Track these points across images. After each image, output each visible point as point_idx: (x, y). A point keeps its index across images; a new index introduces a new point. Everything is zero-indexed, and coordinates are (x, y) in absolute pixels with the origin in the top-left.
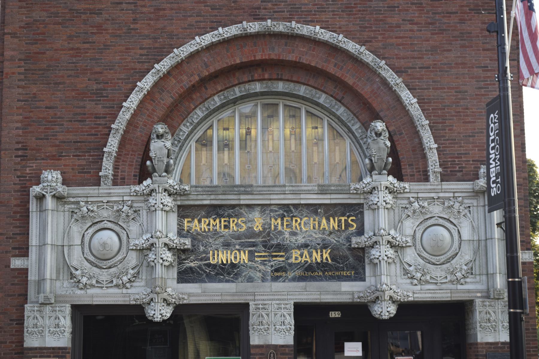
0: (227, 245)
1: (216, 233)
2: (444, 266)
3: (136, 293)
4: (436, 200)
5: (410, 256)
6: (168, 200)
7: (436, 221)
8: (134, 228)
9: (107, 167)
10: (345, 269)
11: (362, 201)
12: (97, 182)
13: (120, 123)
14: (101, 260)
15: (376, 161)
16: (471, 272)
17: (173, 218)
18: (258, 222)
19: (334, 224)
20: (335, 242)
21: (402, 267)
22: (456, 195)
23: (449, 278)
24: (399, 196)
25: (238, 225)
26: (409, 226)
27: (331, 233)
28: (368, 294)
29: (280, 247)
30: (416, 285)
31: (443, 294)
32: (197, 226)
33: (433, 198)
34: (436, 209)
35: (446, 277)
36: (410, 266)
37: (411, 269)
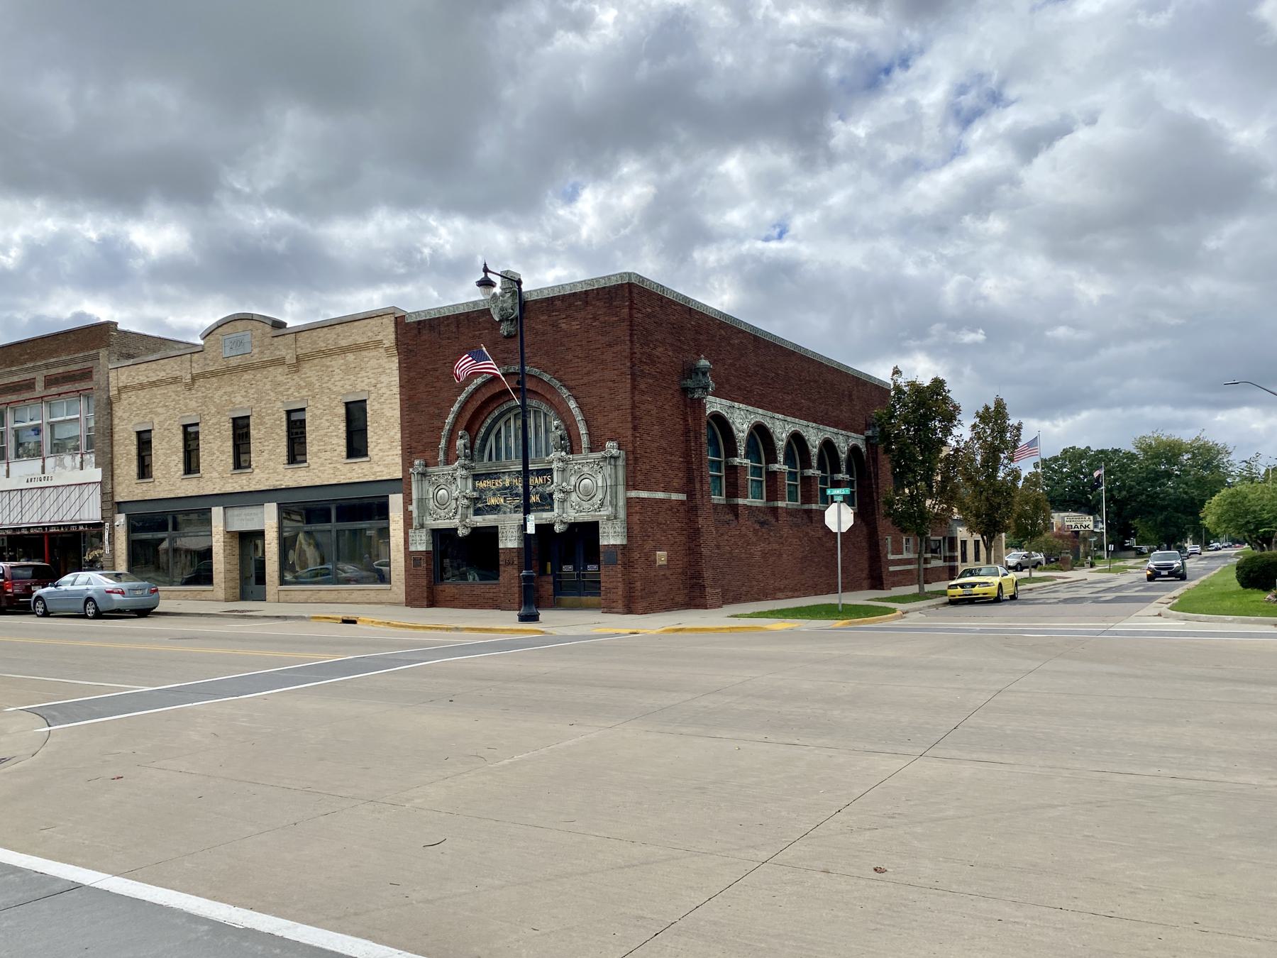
0: (494, 495)
1: (489, 489)
3: (455, 522)
5: (574, 497)
6: (464, 472)
8: (454, 487)
9: (441, 457)
12: (436, 464)
13: (445, 432)
14: (442, 504)
16: (602, 505)
17: (470, 482)
25: (499, 483)
26: (573, 480)
31: (590, 519)
32: (482, 485)
34: (586, 469)
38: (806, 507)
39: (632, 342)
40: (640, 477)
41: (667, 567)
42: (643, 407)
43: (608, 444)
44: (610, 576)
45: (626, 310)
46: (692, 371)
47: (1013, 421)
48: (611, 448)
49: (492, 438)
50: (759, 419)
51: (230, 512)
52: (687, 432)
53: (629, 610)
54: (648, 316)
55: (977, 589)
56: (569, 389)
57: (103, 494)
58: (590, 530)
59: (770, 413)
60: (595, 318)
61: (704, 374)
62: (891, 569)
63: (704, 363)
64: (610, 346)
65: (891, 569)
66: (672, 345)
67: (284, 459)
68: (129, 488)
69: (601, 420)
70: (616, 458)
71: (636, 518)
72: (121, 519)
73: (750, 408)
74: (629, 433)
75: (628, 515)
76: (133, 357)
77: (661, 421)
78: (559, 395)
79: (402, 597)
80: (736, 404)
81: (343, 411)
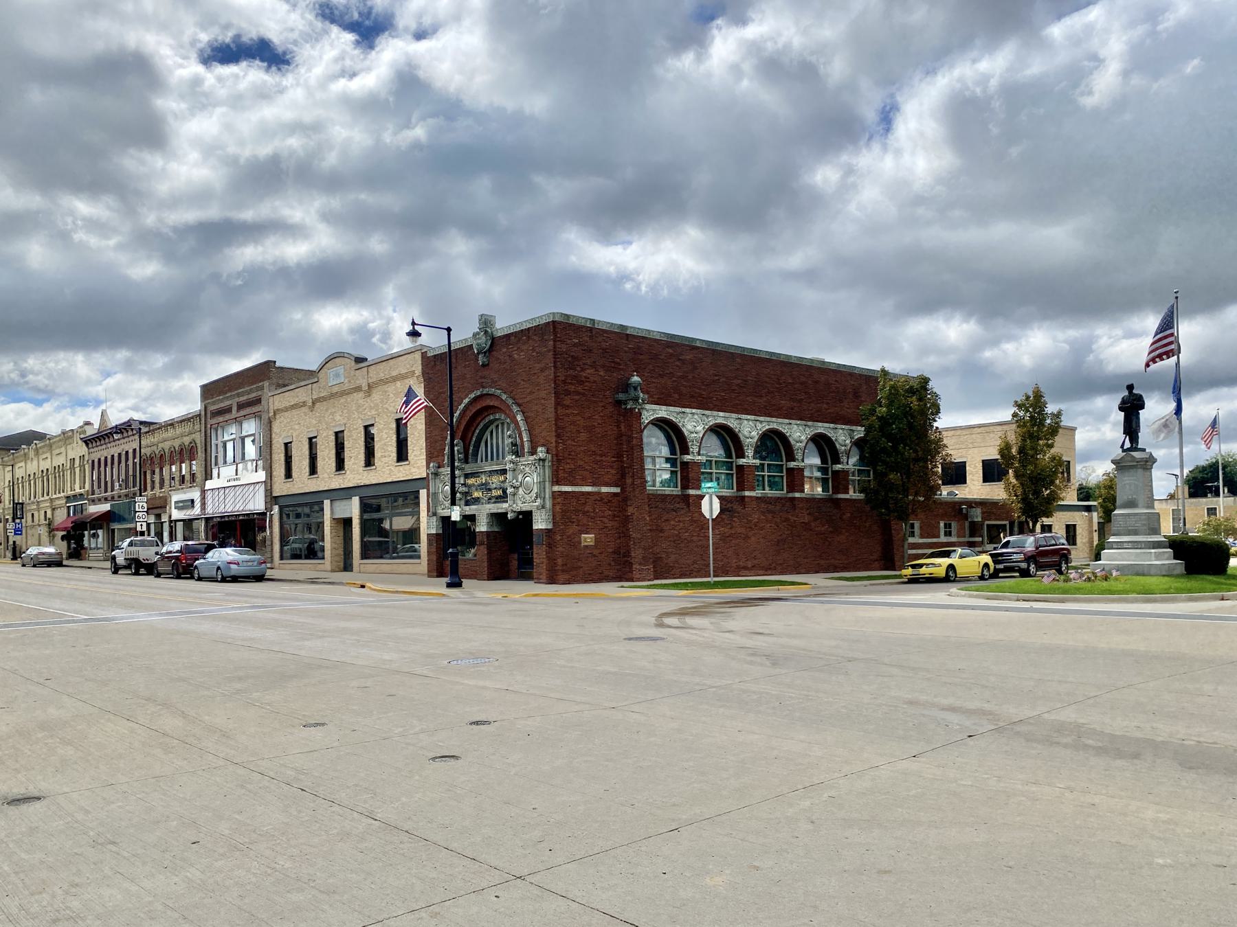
5: (521, 491)
18: (484, 479)
26: (520, 477)
29: (490, 490)
32: (470, 481)
38: (790, 495)
39: (555, 367)
40: (561, 474)
41: (596, 546)
42: (566, 419)
43: (540, 449)
44: (539, 554)
45: (551, 343)
46: (626, 387)
47: (1051, 408)
48: (541, 452)
49: (483, 444)
50: (720, 421)
51: (337, 504)
52: (621, 435)
53: (552, 580)
54: (575, 345)
55: (923, 570)
56: (519, 405)
57: (266, 490)
58: (528, 516)
59: (734, 415)
60: (533, 350)
61: (635, 389)
62: (911, 552)
63: (636, 379)
64: (542, 370)
65: (911, 552)
66: (603, 366)
67: (363, 463)
68: (282, 488)
69: (537, 431)
70: (544, 460)
71: (558, 507)
72: (276, 509)
73: (707, 412)
74: (553, 440)
75: (554, 505)
76: (285, 386)
77: (589, 429)
78: (511, 410)
79: (426, 570)
80: (688, 410)
81: (394, 426)
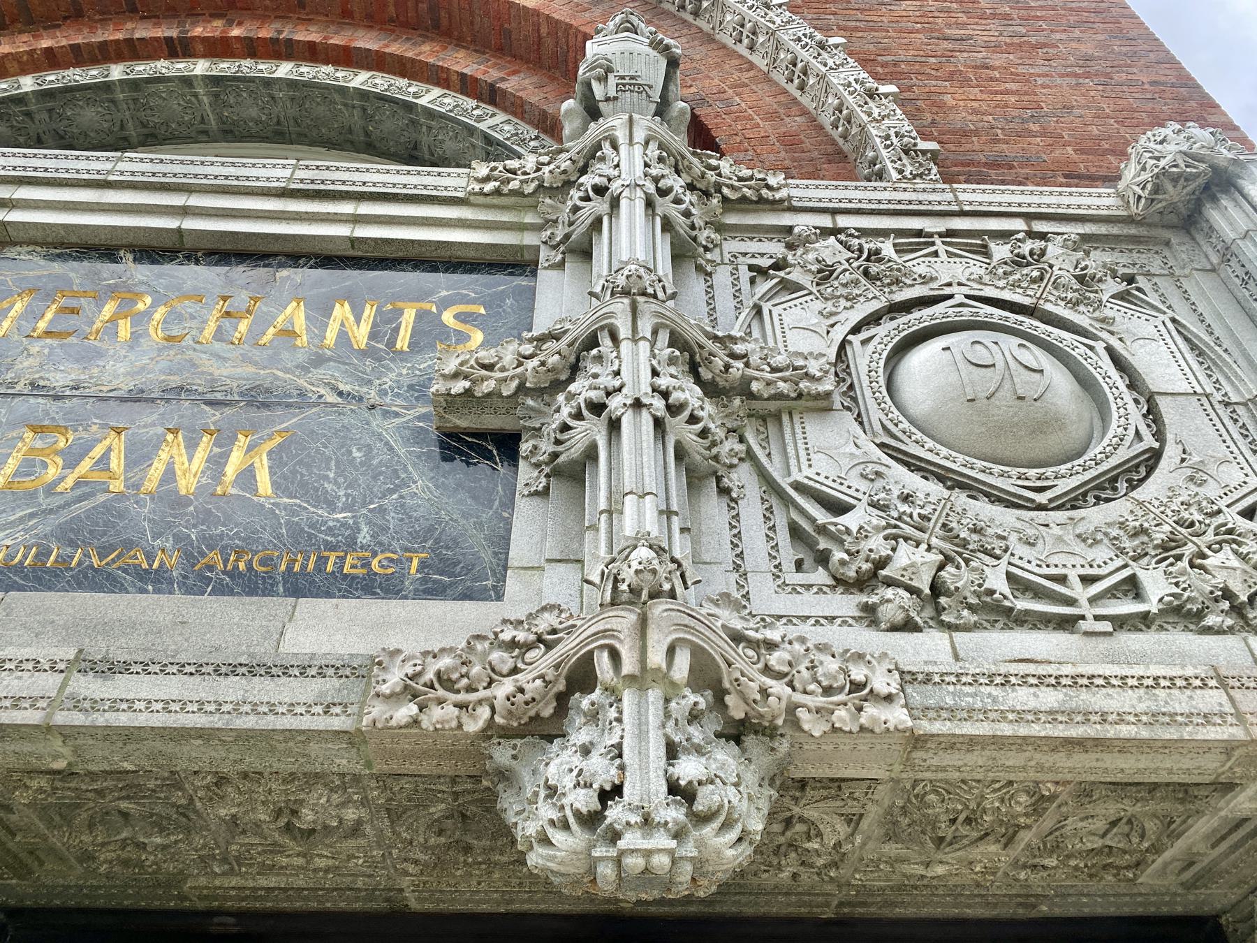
2: (1094, 516)
4: (938, 241)
7: (965, 310)
10: (364, 536)
11: (529, 239)
15: (612, 93)
19: (350, 323)
20: (332, 398)
21: (780, 520)
22: (1039, 226)
23: (1157, 586)
24: (732, 219)
27: (319, 360)
28: (496, 656)
30: (908, 626)
33: (919, 233)
35: (1132, 587)
36: (839, 508)
37: (850, 521)
